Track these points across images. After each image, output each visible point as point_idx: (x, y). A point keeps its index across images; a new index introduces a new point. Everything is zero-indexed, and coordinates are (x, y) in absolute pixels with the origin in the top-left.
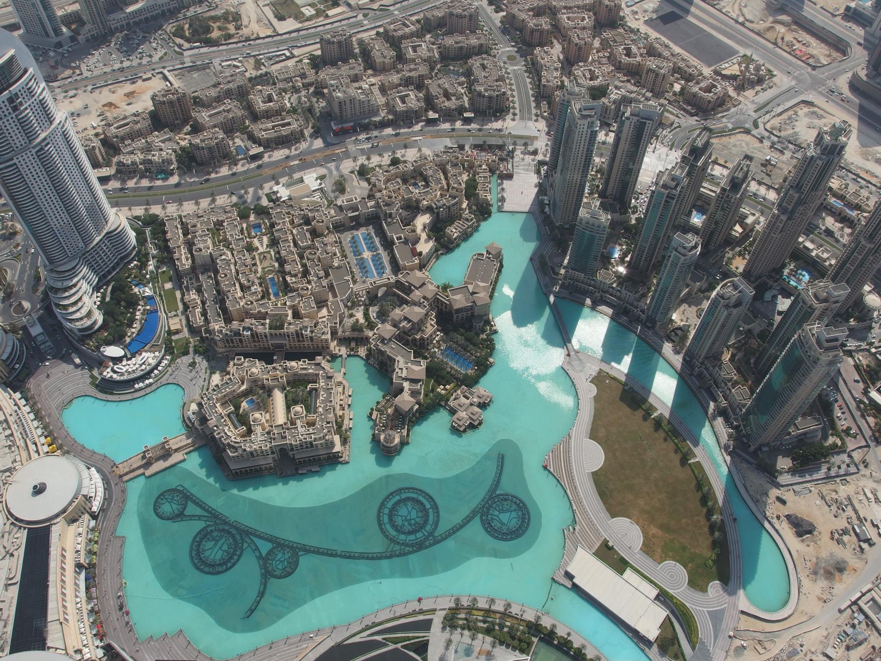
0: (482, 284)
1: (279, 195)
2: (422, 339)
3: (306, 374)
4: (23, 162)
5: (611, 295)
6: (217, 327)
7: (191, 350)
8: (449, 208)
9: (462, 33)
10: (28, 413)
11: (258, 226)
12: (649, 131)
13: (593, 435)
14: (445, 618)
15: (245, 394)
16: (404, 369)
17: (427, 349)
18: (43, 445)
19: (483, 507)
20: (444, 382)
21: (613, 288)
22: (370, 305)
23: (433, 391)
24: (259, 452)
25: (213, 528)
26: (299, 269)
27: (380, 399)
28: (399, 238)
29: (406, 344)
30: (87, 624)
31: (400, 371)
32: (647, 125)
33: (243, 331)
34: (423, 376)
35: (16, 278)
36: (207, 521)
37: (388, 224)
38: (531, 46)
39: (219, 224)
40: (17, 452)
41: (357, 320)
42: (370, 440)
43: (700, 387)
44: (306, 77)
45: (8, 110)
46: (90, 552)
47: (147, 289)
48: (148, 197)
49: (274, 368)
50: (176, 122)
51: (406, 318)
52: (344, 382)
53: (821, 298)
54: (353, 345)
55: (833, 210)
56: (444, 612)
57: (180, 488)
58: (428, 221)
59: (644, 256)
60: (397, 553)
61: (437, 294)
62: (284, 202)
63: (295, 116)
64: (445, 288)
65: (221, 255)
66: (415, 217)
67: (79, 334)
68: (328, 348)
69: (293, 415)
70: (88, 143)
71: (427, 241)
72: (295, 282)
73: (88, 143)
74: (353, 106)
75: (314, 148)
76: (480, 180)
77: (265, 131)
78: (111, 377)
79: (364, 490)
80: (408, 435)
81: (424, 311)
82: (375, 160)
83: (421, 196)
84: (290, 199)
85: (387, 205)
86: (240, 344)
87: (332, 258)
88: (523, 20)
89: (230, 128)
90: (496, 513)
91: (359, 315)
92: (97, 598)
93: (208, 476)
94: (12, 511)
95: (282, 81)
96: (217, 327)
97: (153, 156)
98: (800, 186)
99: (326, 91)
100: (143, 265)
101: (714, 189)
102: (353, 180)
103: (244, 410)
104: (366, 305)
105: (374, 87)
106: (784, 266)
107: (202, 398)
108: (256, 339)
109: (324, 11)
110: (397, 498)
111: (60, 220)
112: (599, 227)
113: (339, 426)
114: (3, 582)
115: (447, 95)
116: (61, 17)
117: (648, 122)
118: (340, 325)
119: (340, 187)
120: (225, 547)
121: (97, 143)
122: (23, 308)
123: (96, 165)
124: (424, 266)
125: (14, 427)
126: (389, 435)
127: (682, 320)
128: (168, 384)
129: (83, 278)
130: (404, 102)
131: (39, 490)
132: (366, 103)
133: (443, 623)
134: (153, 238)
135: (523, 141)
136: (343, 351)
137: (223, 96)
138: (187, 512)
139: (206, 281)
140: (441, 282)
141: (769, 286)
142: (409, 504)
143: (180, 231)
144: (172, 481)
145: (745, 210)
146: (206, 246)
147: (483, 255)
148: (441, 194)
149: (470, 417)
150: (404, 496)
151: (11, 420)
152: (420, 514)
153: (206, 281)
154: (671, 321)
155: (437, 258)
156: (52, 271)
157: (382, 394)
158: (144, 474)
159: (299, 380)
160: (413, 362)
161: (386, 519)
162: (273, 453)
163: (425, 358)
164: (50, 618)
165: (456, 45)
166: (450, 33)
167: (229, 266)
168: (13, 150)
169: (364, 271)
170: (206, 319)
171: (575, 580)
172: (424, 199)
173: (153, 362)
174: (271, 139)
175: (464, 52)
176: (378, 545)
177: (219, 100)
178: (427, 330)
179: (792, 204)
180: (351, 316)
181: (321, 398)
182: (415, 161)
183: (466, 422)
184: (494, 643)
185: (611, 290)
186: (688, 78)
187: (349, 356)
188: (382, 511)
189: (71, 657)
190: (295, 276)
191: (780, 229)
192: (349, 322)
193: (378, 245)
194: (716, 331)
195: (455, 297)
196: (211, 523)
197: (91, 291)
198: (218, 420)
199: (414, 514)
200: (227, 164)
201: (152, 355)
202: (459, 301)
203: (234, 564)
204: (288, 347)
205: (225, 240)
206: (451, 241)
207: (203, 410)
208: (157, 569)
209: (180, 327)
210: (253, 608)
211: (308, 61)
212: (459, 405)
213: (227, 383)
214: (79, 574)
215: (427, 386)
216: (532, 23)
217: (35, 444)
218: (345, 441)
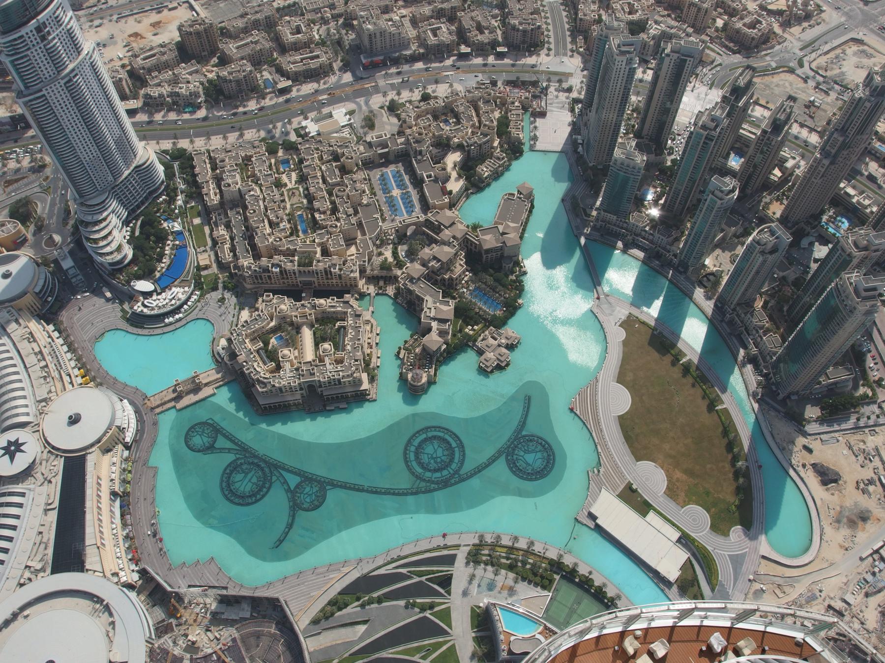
0: (512, 225)
1: (307, 130)
2: (451, 279)
3: (334, 312)
4: (52, 94)
5: (644, 238)
6: (246, 264)
7: (220, 285)
8: (480, 145)
10: (62, 345)
11: (286, 162)
12: (689, 69)
13: (621, 379)
14: (469, 554)
15: (274, 330)
16: (433, 308)
17: (456, 289)
18: (77, 376)
19: (509, 447)
20: (472, 323)
21: (646, 231)
22: (399, 243)
23: (461, 331)
25: (243, 461)
26: (328, 206)
27: (408, 338)
28: (429, 176)
29: (435, 283)
30: (123, 549)
31: (428, 311)
32: (688, 62)
33: (272, 268)
34: (451, 316)
35: (46, 211)
36: (237, 454)
37: (418, 162)
39: (248, 159)
40: (52, 383)
41: (386, 259)
42: (397, 376)
43: (731, 334)
44: (335, 8)
45: (36, 39)
46: (124, 481)
47: (176, 224)
49: (303, 305)
50: (203, 54)
51: (435, 258)
52: (372, 320)
53: (861, 246)
54: (381, 283)
55: (878, 155)
56: (468, 548)
58: (458, 159)
59: (679, 199)
60: (423, 490)
61: (466, 234)
62: (312, 137)
63: (324, 49)
64: (475, 227)
65: (250, 191)
66: (446, 154)
67: (109, 268)
68: (356, 286)
69: (321, 353)
70: (115, 74)
71: (457, 180)
72: (324, 220)
73: (115, 74)
74: (383, 38)
75: (343, 82)
76: (512, 118)
77: (293, 63)
78: (142, 311)
79: (391, 428)
80: (435, 374)
81: (453, 251)
82: (405, 95)
83: (452, 133)
84: (319, 134)
85: (417, 142)
86: (268, 281)
87: (361, 196)
89: (258, 60)
90: (522, 453)
91: (388, 254)
92: (131, 525)
93: (238, 410)
94: (48, 439)
95: (310, 11)
96: (246, 264)
97: (181, 88)
98: (846, 128)
100: (172, 200)
101: (754, 130)
102: (382, 116)
103: (273, 346)
104: (394, 244)
105: (405, 18)
106: (823, 212)
107: (232, 334)
108: (285, 276)
110: (424, 436)
111: (90, 154)
113: (367, 364)
114: (43, 507)
115: (480, 29)
117: (689, 59)
118: (368, 263)
119: (369, 123)
120: (254, 480)
121: (123, 75)
122: (54, 241)
123: (123, 97)
124: (454, 205)
125: (48, 358)
126: (417, 374)
127: (715, 266)
128: (198, 319)
129: (113, 212)
130: (435, 35)
131: (74, 420)
132: (397, 36)
133: (466, 558)
134: (181, 173)
135: (557, 78)
136: (372, 290)
137: (250, 27)
138: (217, 445)
139: (235, 217)
140: (470, 222)
141: (806, 232)
142: (436, 443)
143: (209, 166)
144: (202, 414)
146: (235, 181)
147: (513, 195)
148: (472, 132)
149: (498, 359)
150: (430, 434)
151: (45, 351)
152: (446, 453)
153: (235, 217)
154: (704, 266)
155: (468, 197)
156: (82, 204)
157: (409, 333)
158: (174, 407)
159: (328, 318)
160: (441, 302)
161: (412, 456)
162: (301, 389)
163: (454, 298)
164: (88, 542)
167: (258, 202)
168: (42, 81)
169: (393, 209)
170: (235, 255)
171: (598, 521)
172: (455, 137)
173: (183, 297)
174: (300, 72)
176: (404, 481)
177: (246, 31)
178: (456, 270)
179: (836, 148)
180: (380, 254)
181: (350, 336)
182: (446, 97)
183: (493, 363)
184: (517, 579)
185: (643, 233)
187: (377, 294)
188: (408, 448)
189: (109, 579)
190: (324, 213)
191: (821, 173)
192: (377, 261)
193: (408, 183)
194: (750, 278)
196: (241, 456)
197: (121, 225)
198: (248, 356)
199: (440, 452)
200: (254, 97)
201: (182, 290)
202: (489, 241)
203: (263, 496)
204: (316, 284)
206: (481, 180)
208: (188, 498)
209: (209, 263)
210: (282, 539)
212: (487, 346)
213: (256, 319)
214: (114, 501)
215: (455, 326)
217: (69, 375)
218: (372, 379)
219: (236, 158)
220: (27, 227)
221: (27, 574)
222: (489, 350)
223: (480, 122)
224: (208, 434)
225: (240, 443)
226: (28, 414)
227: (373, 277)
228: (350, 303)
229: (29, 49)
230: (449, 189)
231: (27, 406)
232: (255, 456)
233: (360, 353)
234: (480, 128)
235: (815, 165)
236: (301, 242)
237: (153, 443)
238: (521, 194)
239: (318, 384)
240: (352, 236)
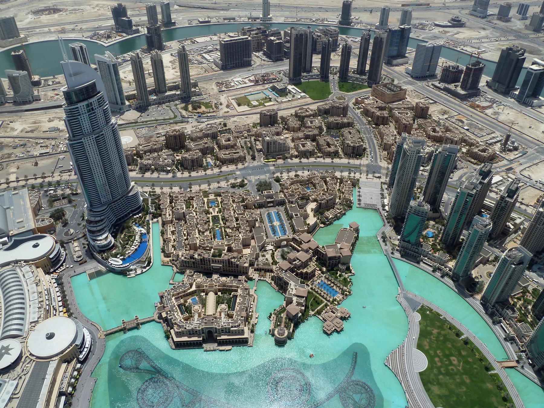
3: (231, 286)
4: (87, 142)
6: (180, 254)
8: (328, 201)
9: (339, 116)
11: (212, 201)
13: (420, 347)
21: (429, 254)
24: (194, 331)
26: (234, 226)
29: (297, 275)
41: (267, 260)
44: (250, 132)
50: (176, 148)
51: (298, 259)
52: (255, 295)
57: (140, 351)
58: (314, 207)
61: (318, 247)
66: (307, 204)
67: (98, 249)
68: (247, 273)
77: (224, 155)
82: (285, 176)
83: (311, 193)
85: (291, 195)
86: (193, 265)
88: (373, 112)
89: (205, 151)
95: (236, 132)
99: (260, 139)
101: (493, 202)
111: (101, 181)
115: (329, 145)
116: (126, 96)
131: (50, 336)
132: (282, 145)
134: (151, 203)
136: (256, 276)
143: (169, 201)
145: (513, 215)
146: (182, 207)
147: (347, 229)
148: (323, 194)
166: (332, 115)
168: (83, 134)
174: (227, 159)
175: (339, 126)
177: (201, 138)
182: (308, 175)
186: (471, 145)
190: (232, 229)
202: (331, 253)
204: (222, 270)
216: (378, 113)
219: (185, 197)
223: (327, 189)
229: (80, 115)
235: (538, 216)
238: (351, 228)
240: (247, 243)
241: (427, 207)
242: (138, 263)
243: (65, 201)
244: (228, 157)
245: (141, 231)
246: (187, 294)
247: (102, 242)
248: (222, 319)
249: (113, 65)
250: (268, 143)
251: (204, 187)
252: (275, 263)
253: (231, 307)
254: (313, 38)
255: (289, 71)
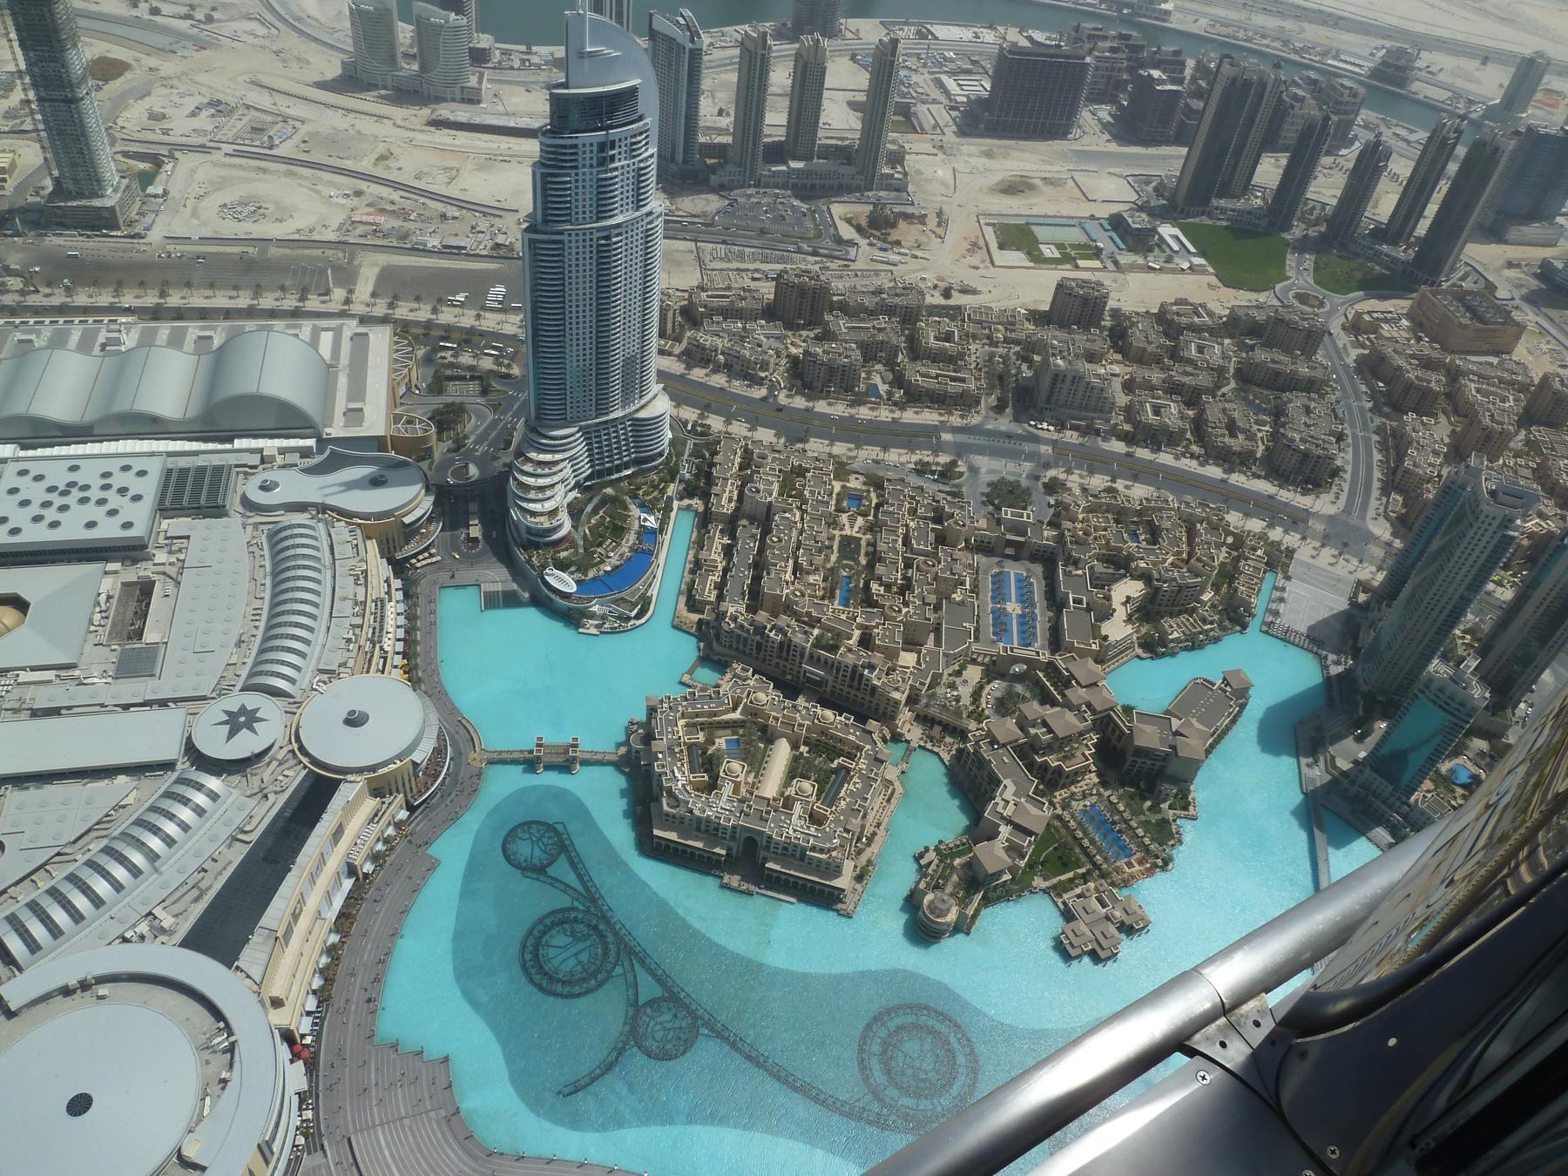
2: (1059, 770)
3: (841, 740)
6: (731, 610)
8: (1180, 588)
9: (1288, 351)
11: (857, 497)
18: (396, 667)
25: (580, 916)
29: (1030, 766)
34: (1039, 829)
36: (577, 900)
38: (1399, 409)
40: (354, 654)
41: (958, 699)
42: (905, 893)
47: (652, 518)
48: (709, 401)
49: (794, 707)
51: (1045, 724)
52: (897, 784)
54: (937, 729)
57: (560, 828)
61: (1112, 709)
64: (1128, 710)
66: (1115, 579)
67: (525, 536)
68: (893, 718)
73: (665, 298)
77: (922, 375)
80: (975, 916)
81: (1082, 726)
82: (1074, 481)
83: (1139, 552)
86: (754, 652)
87: (956, 587)
88: (1399, 368)
89: (871, 352)
96: (731, 610)
99: (1037, 358)
103: (718, 750)
105: (1115, 379)
108: (784, 654)
109: (1075, 259)
112: (1462, 704)
115: (1232, 428)
120: (584, 957)
122: (467, 473)
123: (662, 335)
129: (571, 459)
131: (355, 720)
134: (690, 456)
136: (914, 734)
138: (551, 871)
143: (738, 460)
147: (1213, 684)
148: (1172, 564)
149: (1097, 940)
151: (371, 606)
162: (733, 838)
165: (1271, 365)
166: (1268, 345)
174: (928, 390)
177: (872, 313)
182: (1147, 499)
189: (262, 1002)
190: (888, 587)
195: (1142, 726)
197: (573, 483)
202: (1148, 737)
204: (829, 689)
205: (800, 495)
206: (1163, 641)
207: (653, 721)
208: (459, 936)
211: (1023, 311)
213: (711, 698)
217: (385, 659)
218: (859, 878)
220: (440, 439)
221: (143, 928)
222: (1087, 918)
223: (1190, 555)
224: (546, 846)
225: (589, 884)
226: (292, 681)
227: (925, 716)
228: (875, 737)
229: (576, 167)
230: (1104, 633)
231: (298, 669)
232: (604, 918)
233: (858, 821)
234: (1187, 562)
236: (834, 610)
237: (453, 818)
238: (1228, 684)
239: (764, 843)
241: (1479, 693)
242: (615, 602)
243: (474, 387)
244: (931, 384)
245: (645, 520)
246: (719, 723)
247: (537, 520)
248: (794, 818)
249: (690, 50)
250: (1058, 377)
251: (840, 449)
252: (978, 716)
253: (828, 793)
254: (1280, 100)
255: (1178, 183)
